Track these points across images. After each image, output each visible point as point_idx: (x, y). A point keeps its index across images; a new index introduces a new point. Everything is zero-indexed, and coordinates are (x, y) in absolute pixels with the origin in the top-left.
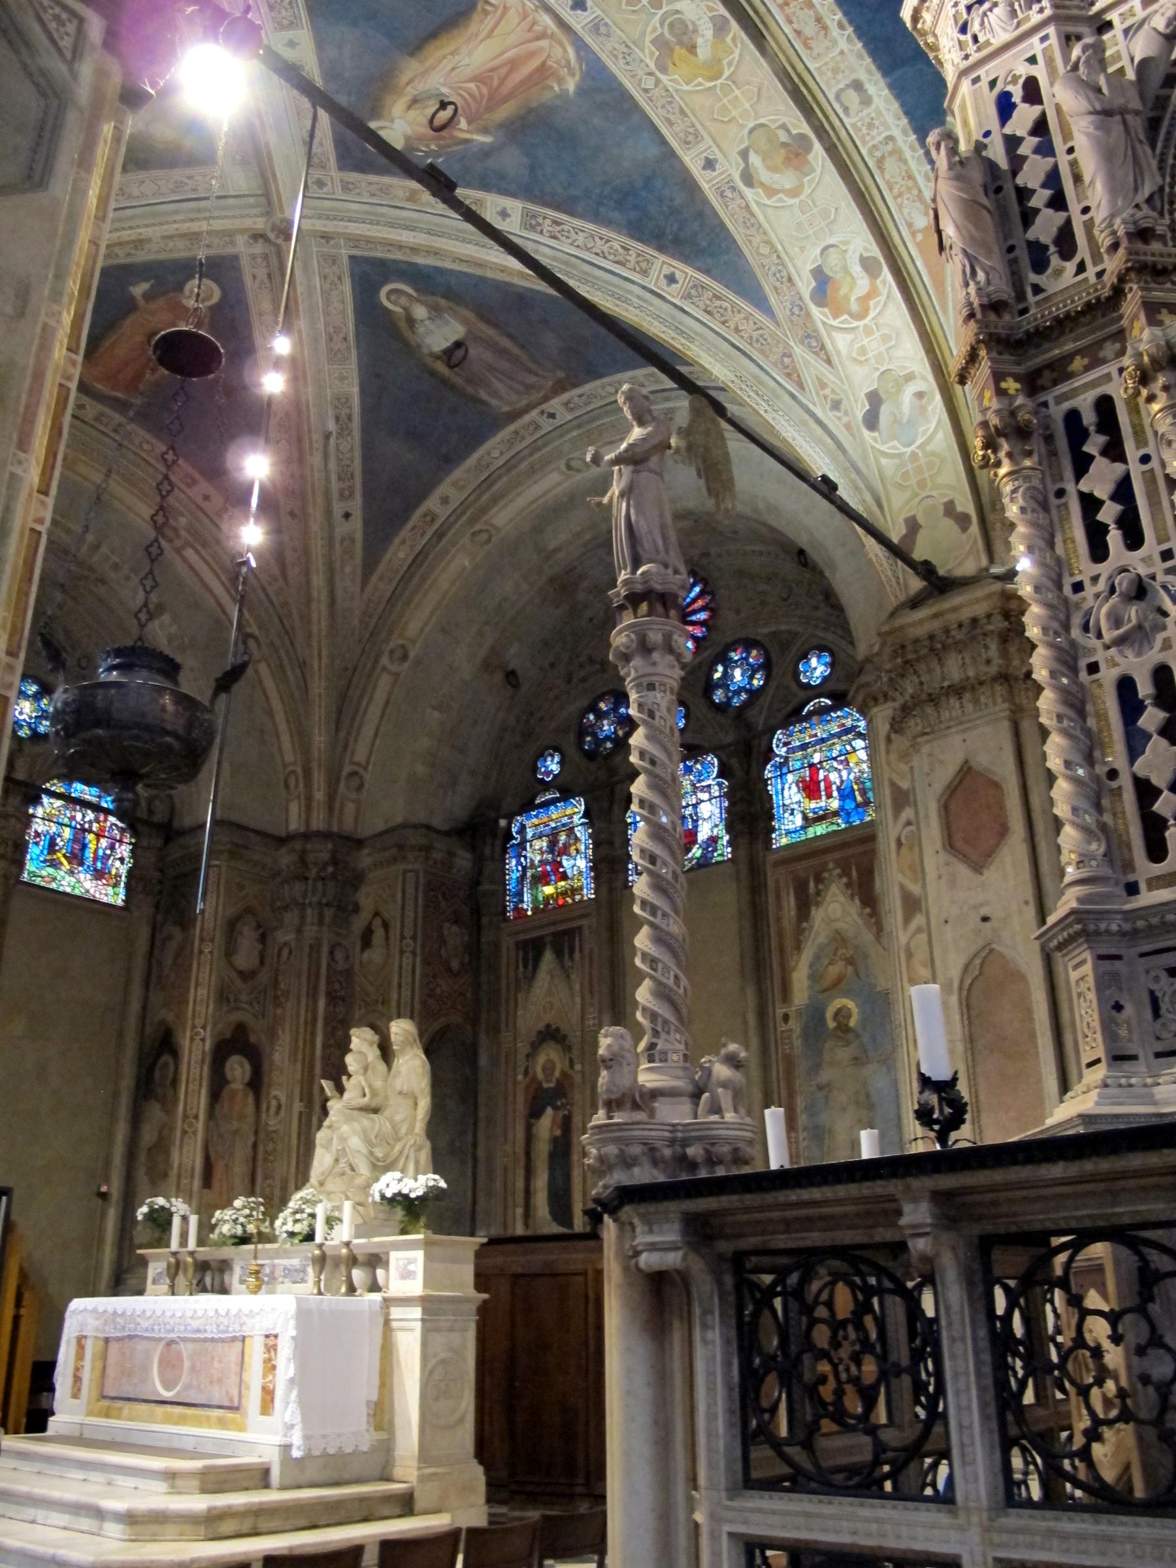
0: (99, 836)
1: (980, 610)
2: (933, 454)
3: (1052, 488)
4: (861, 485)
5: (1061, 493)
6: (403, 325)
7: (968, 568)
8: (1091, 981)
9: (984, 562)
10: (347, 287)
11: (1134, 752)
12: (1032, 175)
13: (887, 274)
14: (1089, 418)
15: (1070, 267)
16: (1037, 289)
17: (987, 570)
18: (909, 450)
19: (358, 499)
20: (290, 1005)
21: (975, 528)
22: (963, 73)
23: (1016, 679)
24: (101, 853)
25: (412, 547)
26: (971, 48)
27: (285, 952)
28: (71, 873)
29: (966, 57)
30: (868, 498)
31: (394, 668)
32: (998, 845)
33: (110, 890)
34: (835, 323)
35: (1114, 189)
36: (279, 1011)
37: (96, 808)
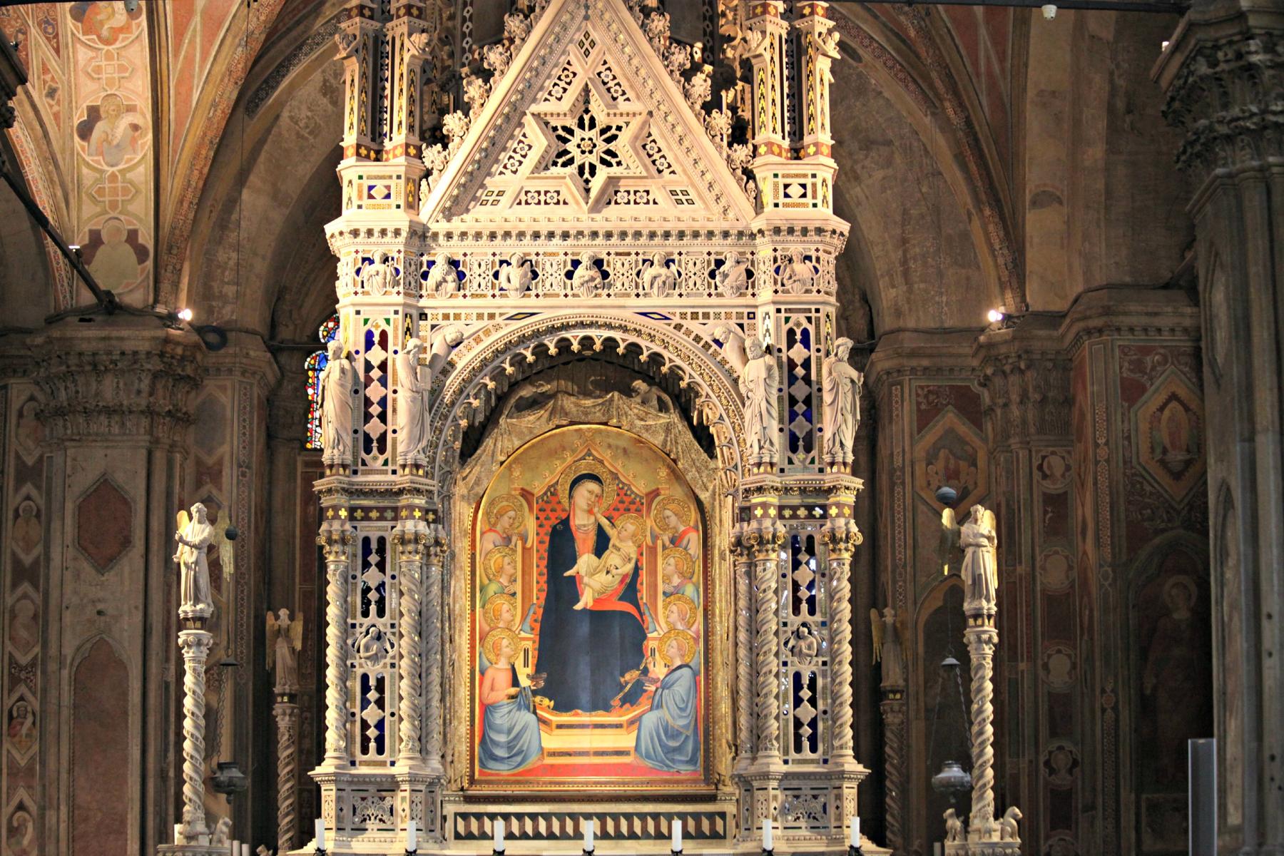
1: (144, 347)
2: (131, 183)
3: (351, 573)
4: (56, 178)
5: (354, 577)
7: (135, 298)
8: (334, 798)
9: (151, 300)
11: (363, 708)
12: (375, 392)
13: (143, 19)
14: (374, 546)
15: (382, 458)
16: (364, 464)
17: (153, 307)
18: (111, 170)
21: (150, 263)
22: (354, 305)
23: (158, 414)
26: (359, 290)
29: (356, 293)
30: (59, 193)
32: (120, 553)
34: (83, 38)
35: (410, 438)
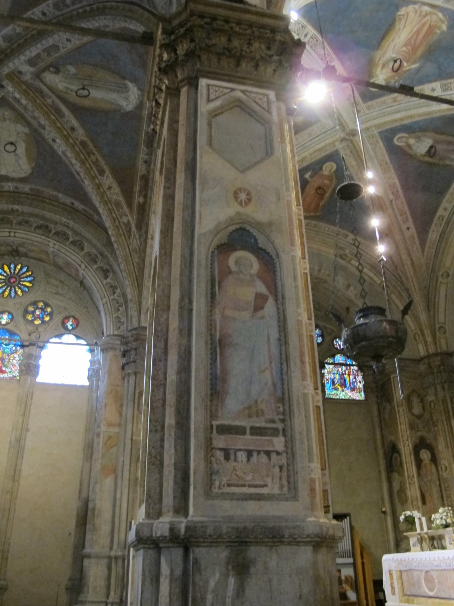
0: (349, 375)
6: (407, 149)
10: (381, 144)
19: (410, 220)
20: (440, 426)
24: (351, 381)
25: (438, 232)
27: (432, 404)
28: (343, 391)
31: (445, 281)
33: (358, 394)
36: (436, 428)
37: (346, 365)
